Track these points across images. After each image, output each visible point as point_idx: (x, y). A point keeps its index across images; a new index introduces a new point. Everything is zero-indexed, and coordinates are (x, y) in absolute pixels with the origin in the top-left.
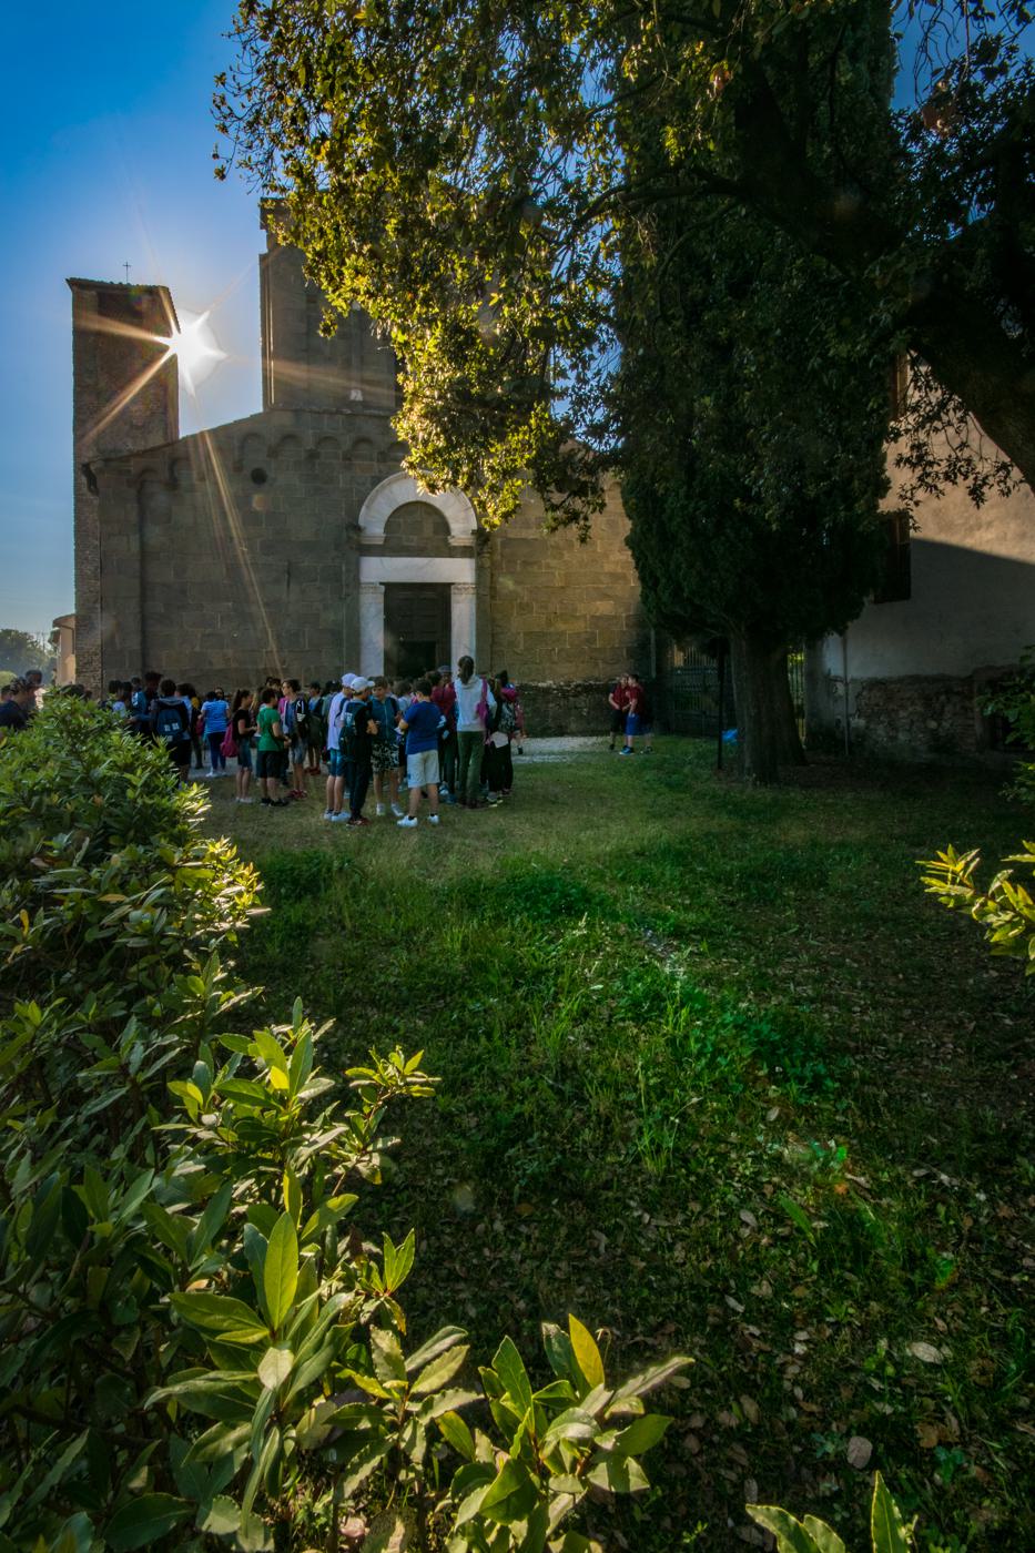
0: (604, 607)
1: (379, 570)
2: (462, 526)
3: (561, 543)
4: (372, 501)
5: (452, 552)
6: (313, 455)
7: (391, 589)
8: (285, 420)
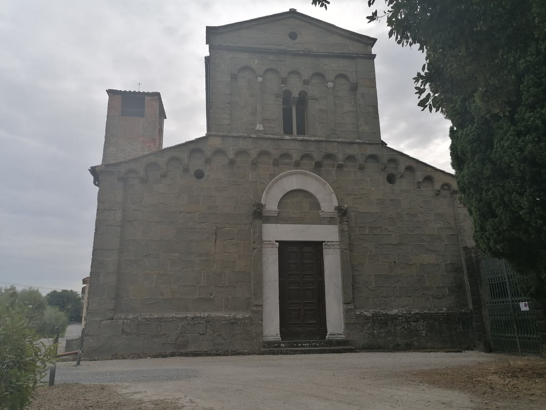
0: (429, 258)
2: (328, 203)
6: (232, 163)
7: (284, 246)
8: (216, 142)
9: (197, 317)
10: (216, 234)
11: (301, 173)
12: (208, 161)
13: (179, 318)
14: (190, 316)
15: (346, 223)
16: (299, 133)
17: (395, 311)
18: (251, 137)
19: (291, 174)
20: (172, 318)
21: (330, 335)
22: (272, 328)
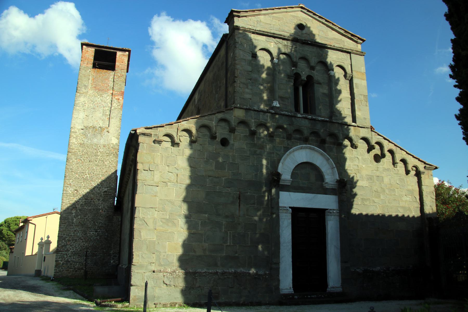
1: (289, 200)
3: (379, 190)
4: (285, 160)
5: (325, 191)
7: (296, 211)
9: (226, 273)
10: (239, 198)
11: (310, 148)
12: (232, 130)
13: (211, 273)
14: (220, 271)
15: (345, 194)
16: (306, 111)
17: (378, 268)
18: (270, 113)
19: (302, 148)
20: (205, 273)
21: (331, 288)
22: (286, 282)
